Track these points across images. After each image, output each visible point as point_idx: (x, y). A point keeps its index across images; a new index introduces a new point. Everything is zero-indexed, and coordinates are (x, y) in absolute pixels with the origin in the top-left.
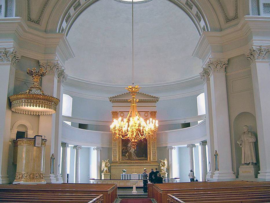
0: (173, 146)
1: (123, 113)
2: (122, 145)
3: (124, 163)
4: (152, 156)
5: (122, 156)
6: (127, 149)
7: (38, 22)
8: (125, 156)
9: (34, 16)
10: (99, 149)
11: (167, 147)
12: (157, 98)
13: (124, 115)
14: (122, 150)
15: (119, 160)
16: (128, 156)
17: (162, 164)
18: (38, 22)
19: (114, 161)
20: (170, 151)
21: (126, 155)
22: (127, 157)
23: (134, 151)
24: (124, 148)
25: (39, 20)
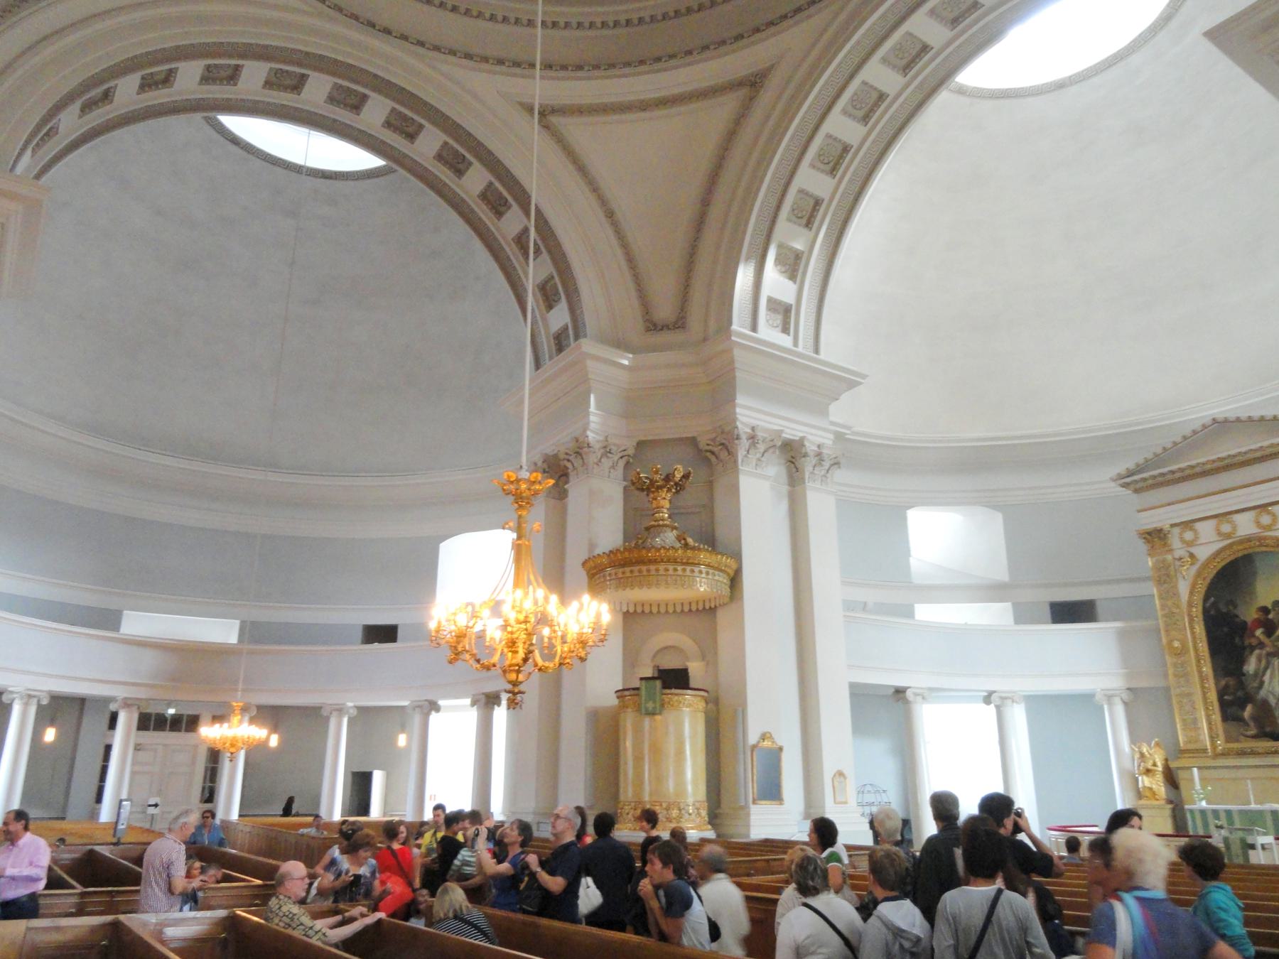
1: (1192, 529)
2: (1215, 670)
3: (1242, 753)
5: (1226, 718)
6: (1241, 685)
7: (679, 324)
8: (1240, 719)
9: (664, 312)
13: (1196, 538)
14: (1221, 694)
15: (1212, 739)
18: (679, 324)
22: (1252, 724)
24: (1226, 686)
25: (681, 315)
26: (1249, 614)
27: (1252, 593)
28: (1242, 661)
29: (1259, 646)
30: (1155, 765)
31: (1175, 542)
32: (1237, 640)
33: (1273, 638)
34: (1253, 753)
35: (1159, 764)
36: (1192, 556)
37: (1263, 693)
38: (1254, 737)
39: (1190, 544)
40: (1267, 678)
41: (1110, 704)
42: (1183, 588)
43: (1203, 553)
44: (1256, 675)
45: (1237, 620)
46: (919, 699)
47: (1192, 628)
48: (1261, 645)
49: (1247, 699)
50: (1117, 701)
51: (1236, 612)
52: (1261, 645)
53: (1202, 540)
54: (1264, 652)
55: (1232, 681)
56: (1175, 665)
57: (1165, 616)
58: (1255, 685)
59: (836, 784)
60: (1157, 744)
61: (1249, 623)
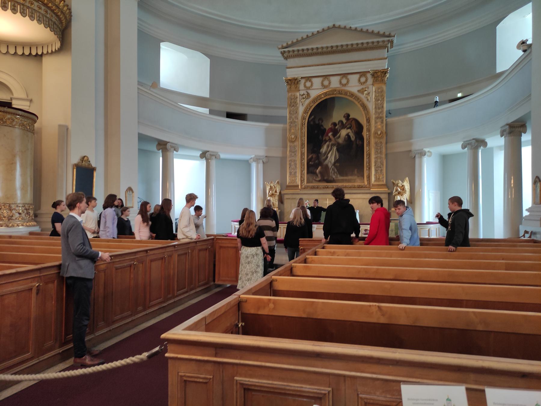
0: (425, 149)
1: (310, 81)
3: (313, 188)
4: (373, 172)
5: (308, 173)
6: (318, 158)
8: (314, 173)
10: (260, 159)
11: (410, 151)
12: (389, 36)
13: (312, 85)
15: (302, 181)
16: (320, 172)
17: (397, 190)
19: (292, 184)
20: (417, 160)
21: (318, 171)
22: (319, 175)
23: (335, 163)
24: (312, 157)
26: (328, 125)
27: (331, 116)
28: (320, 147)
29: (329, 141)
30: (276, 192)
31: (302, 86)
32: (320, 137)
33: (335, 137)
34: (318, 188)
35: (278, 192)
36: (308, 94)
37: (326, 162)
38: (320, 181)
39: (309, 88)
40: (329, 155)
41: (258, 163)
42: (301, 110)
43: (314, 94)
44: (325, 153)
45: (322, 128)
46: (172, 149)
47: (302, 129)
48: (330, 140)
49: (320, 164)
50: (261, 161)
51: (322, 124)
52: (330, 140)
53: (313, 88)
54: (331, 143)
55: (314, 156)
56: (290, 147)
57: (291, 123)
58: (324, 158)
59: (128, 195)
60: (278, 183)
61: (327, 129)
